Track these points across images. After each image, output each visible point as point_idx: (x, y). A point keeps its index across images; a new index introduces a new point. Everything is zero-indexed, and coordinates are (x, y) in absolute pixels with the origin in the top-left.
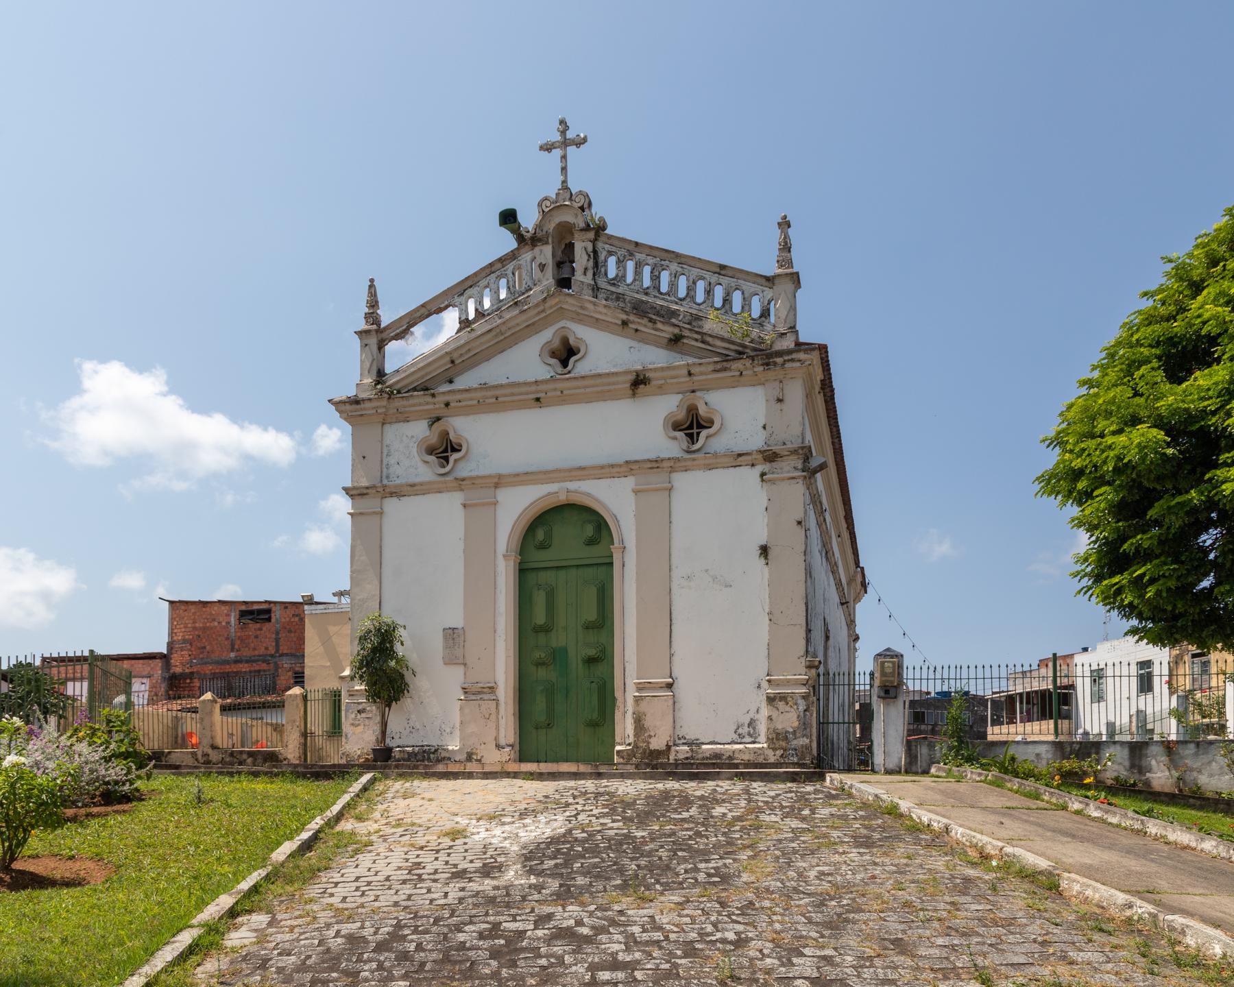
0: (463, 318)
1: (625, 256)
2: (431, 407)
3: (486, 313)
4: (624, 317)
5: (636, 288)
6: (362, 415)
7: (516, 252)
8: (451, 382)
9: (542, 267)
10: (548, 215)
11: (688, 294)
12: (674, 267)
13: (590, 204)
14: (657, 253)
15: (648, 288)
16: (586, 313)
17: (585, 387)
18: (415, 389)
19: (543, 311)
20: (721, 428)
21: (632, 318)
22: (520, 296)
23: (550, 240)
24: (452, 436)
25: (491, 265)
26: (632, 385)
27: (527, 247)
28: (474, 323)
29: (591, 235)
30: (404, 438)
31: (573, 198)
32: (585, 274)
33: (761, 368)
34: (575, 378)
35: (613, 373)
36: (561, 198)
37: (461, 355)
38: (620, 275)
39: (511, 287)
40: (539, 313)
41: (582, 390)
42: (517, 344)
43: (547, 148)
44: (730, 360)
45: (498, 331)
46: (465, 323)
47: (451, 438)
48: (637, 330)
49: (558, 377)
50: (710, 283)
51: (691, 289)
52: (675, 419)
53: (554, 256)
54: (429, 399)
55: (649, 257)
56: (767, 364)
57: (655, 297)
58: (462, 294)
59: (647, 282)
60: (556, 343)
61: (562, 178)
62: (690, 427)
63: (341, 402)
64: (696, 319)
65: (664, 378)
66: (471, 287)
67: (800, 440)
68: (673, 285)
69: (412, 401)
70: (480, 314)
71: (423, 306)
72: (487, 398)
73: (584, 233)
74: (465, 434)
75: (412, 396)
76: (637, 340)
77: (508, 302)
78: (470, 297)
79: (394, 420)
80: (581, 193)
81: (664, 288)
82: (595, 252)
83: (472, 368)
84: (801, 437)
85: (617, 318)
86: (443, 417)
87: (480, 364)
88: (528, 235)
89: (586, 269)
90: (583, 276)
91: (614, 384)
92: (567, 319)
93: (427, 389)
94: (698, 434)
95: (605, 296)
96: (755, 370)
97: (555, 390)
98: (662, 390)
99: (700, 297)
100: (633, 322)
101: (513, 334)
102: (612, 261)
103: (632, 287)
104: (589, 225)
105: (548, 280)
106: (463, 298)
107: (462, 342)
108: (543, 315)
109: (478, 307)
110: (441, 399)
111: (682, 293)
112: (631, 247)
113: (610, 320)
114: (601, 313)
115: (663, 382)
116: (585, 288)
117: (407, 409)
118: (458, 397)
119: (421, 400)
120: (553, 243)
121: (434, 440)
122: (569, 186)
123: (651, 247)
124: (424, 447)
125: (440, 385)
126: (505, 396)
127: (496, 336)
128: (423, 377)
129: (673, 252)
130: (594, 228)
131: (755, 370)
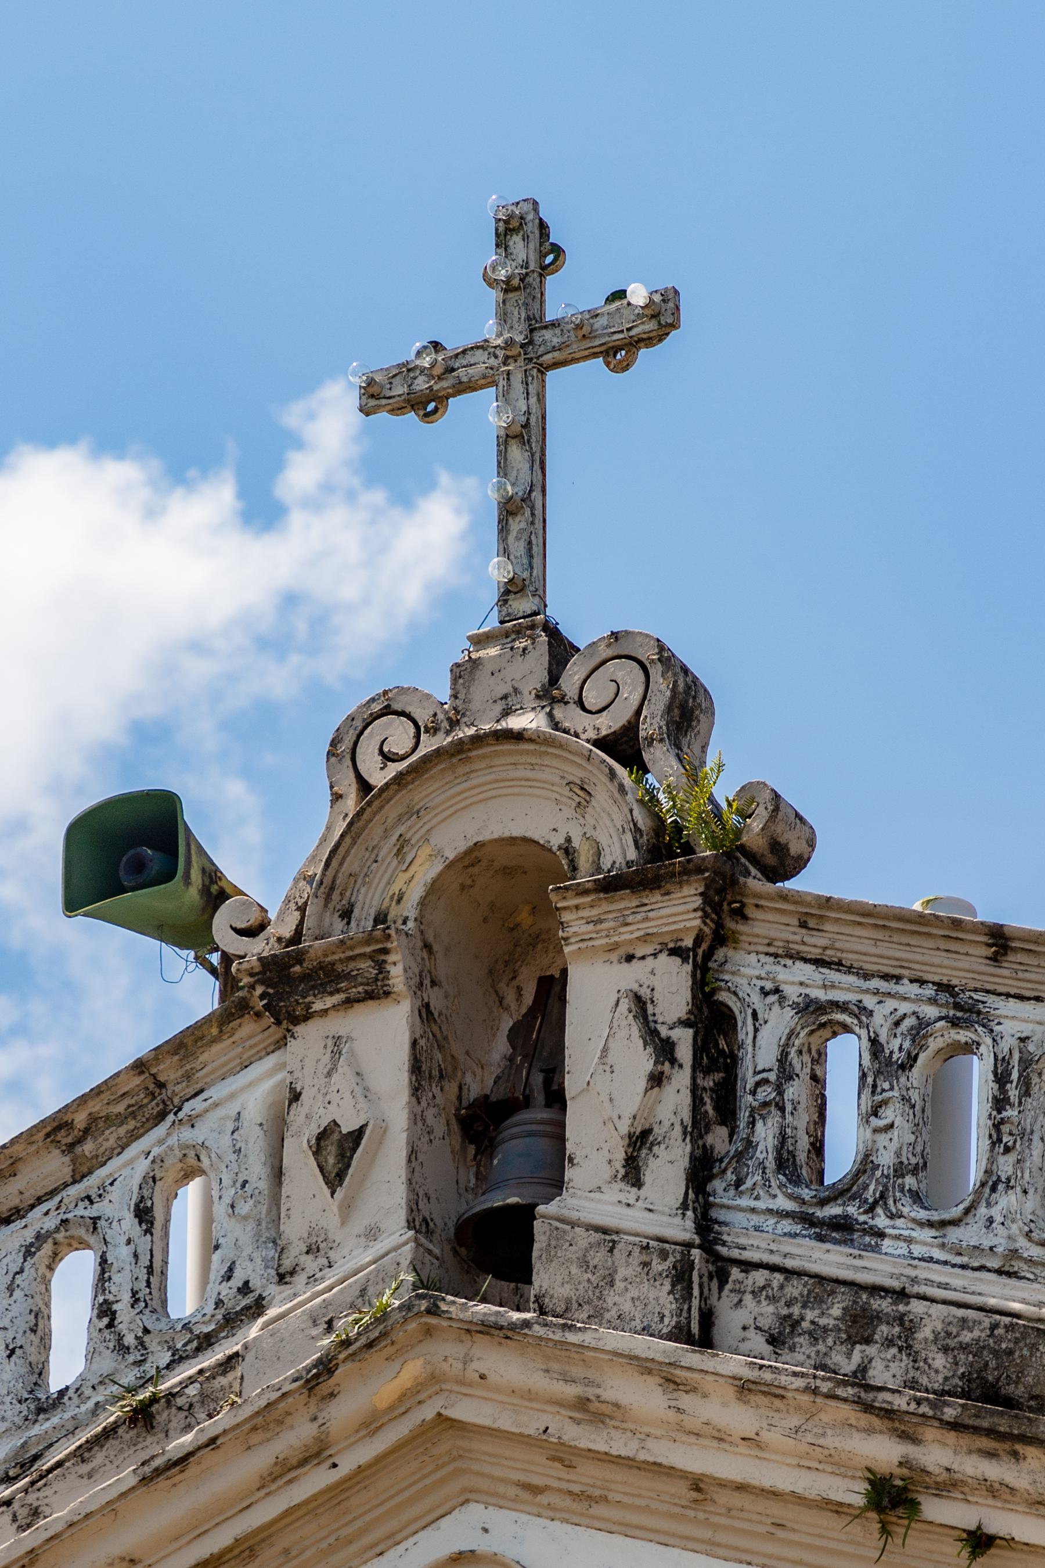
1: (920, 1031)
7: (168, 1071)
10: (392, 810)
16: (620, 1445)
22: (178, 1359)
23: (397, 974)
38: (886, 1159)
39: (123, 1308)
73: (626, 901)
92: (494, 1499)
95: (767, 1313)
105: (372, 1234)
116: (627, 1269)
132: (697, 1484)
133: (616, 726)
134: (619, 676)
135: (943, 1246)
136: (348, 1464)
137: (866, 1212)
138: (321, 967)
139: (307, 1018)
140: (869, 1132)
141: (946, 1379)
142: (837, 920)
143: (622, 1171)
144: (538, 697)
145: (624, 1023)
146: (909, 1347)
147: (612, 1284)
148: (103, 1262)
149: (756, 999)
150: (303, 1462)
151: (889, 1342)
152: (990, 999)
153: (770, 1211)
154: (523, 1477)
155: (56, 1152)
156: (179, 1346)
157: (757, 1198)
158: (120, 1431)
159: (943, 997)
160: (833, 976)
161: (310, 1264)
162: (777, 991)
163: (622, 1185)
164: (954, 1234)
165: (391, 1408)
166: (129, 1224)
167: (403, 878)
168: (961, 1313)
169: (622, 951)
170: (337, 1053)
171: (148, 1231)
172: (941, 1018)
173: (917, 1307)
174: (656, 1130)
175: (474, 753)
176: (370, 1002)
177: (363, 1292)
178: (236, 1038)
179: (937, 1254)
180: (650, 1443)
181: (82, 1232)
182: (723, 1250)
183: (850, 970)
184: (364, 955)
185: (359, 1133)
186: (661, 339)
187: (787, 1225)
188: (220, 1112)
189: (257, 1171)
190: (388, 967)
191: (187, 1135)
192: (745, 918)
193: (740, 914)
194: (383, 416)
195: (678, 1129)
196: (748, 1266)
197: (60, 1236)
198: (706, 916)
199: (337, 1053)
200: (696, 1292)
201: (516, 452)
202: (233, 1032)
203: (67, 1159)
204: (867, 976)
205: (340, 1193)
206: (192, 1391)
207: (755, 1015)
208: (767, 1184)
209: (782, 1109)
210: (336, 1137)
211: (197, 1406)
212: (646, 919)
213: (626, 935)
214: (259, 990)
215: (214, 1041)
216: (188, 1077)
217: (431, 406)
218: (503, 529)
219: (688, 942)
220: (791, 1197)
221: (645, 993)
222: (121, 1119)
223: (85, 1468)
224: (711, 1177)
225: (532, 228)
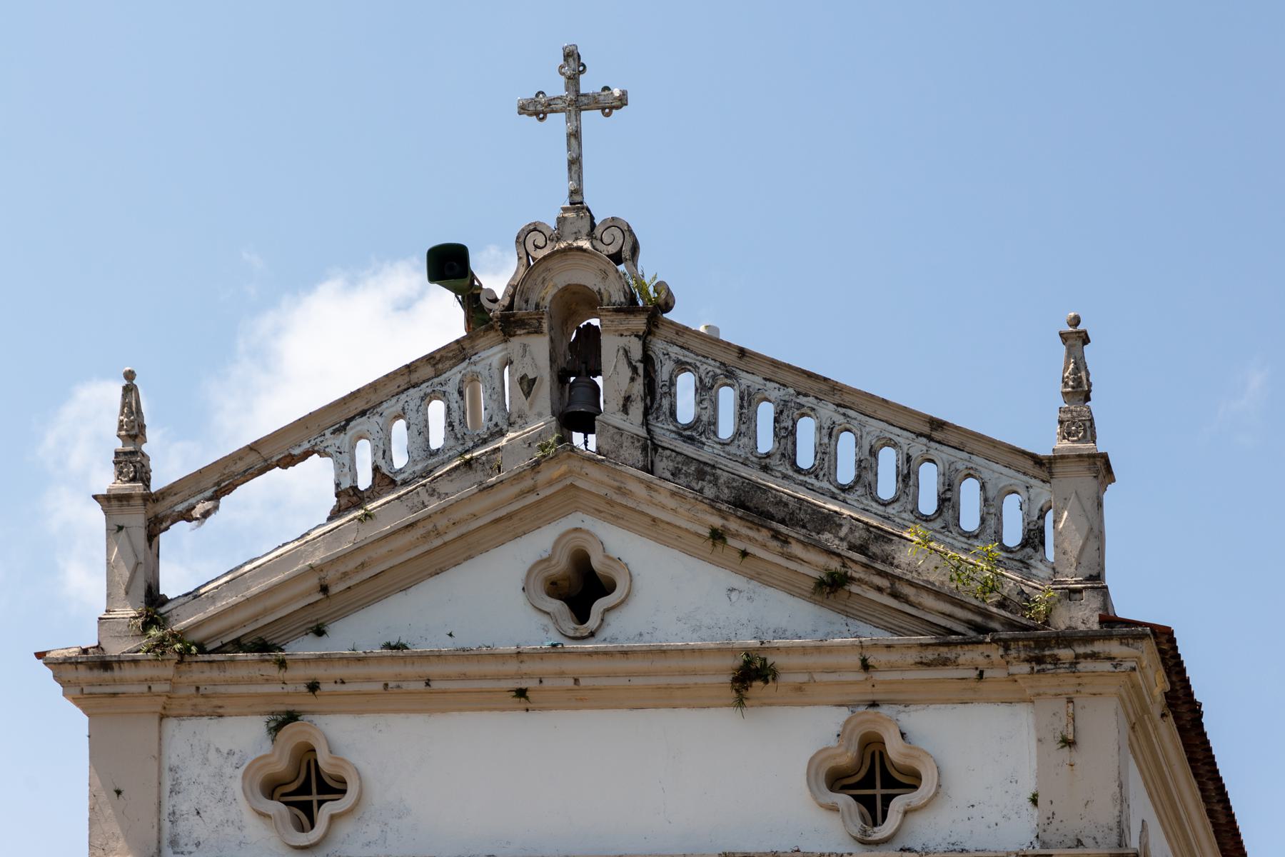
0: (346, 484)
1: (715, 377)
2: (276, 688)
3: (399, 479)
4: (717, 522)
5: (742, 452)
6: (114, 695)
7: (467, 345)
8: (320, 632)
9: (527, 385)
11: (858, 477)
12: (828, 411)
13: (635, 249)
14: (789, 378)
15: (768, 455)
16: (631, 504)
17: (630, 674)
18: (238, 645)
19: (532, 490)
20: (936, 794)
21: (733, 525)
22: (476, 446)
23: (545, 326)
24: (323, 759)
25: (410, 368)
26: (735, 680)
27: (492, 334)
28: (372, 500)
29: (639, 323)
30: (212, 755)
31: (598, 232)
32: (625, 409)
33: (1025, 668)
34: (606, 653)
35: (693, 650)
36: (568, 229)
37: (345, 574)
38: (705, 419)
39: (456, 424)
40: (523, 494)
41: (622, 682)
42: (470, 557)
43: (537, 109)
44: (956, 644)
45: (430, 527)
46: (349, 498)
47: (321, 763)
48: (744, 554)
49: (571, 645)
50: (909, 458)
51: (866, 466)
52: (832, 764)
53: (553, 360)
54: (273, 671)
55: (770, 385)
56: (1040, 660)
57: (785, 477)
58: (342, 429)
59: (766, 442)
60: (561, 565)
61: (572, 185)
62: (868, 782)
63: (67, 661)
64: (877, 538)
65: (809, 671)
66: (363, 413)
67: (1114, 838)
68: (826, 454)
69: (231, 673)
70: (384, 479)
71: (253, 448)
72: (406, 679)
73: (622, 316)
74: (353, 758)
75: (232, 661)
76: (744, 574)
77: (450, 459)
78: (361, 438)
79: (189, 712)
80: (613, 223)
81: (806, 459)
82: (647, 359)
83: (368, 604)
84: (1116, 831)
85: (701, 523)
86: (301, 713)
87: (386, 596)
88: (496, 310)
89: (627, 399)
90: (620, 415)
91: (694, 673)
93: (263, 646)
94: (887, 800)
95: (671, 465)
96: (1013, 669)
97: (561, 674)
98: (801, 695)
99: (887, 487)
100: (736, 535)
101: (461, 537)
102: (686, 385)
103: (732, 449)
104: (633, 300)
106: (343, 440)
107: (347, 546)
108: (532, 498)
109: (381, 463)
110: (301, 674)
111: (846, 473)
112: (731, 359)
113: (684, 524)
114: (664, 507)
115: (803, 678)
117: (222, 689)
118: (339, 671)
119: (255, 672)
120: (551, 329)
121: (281, 765)
122: (588, 202)
123: (775, 364)
124: (259, 779)
125: (296, 636)
126: (447, 678)
127: (425, 537)
128: (255, 618)
129: (826, 379)
130: (644, 310)
131: (1013, 669)
132: (654, 520)
133: (614, 251)
134: (615, 233)
135: (724, 451)
136: (542, 495)
137: (699, 435)
138: (520, 320)
139: (514, 336)
140: (699, 409)
141: (728, 497)
142: (688, 335)
143: (622, 409)
144: (587, 235)
145: (621, 358)
146: (716, 485)
147: (622, 447)
148: (449, 411)
149: (661, 355)
150: (528, 492)
151: (710, 482)
152: (738, 371)
153: (668, 429)
154: (597, 507)
155: (430, 366)
156: (476, 440)
157: (663, 424)
158: (461, 467)
159: (722, 367)
160: (687, 353)
161: (520, 422)
162: (668, 354)
163: (621, 413)
164: (727, 448)
165: (557, 479)
166: (456, 395)
167: (544, 292)
168: (733, 476)
169: (619, 332)
170: (525, 351)
171: (462, 399)
172: (722, 374)
173: (719, 472)
174: (632, 396)
175: (569, 253)
176: (536, 334)
177: (540, 435)
178: (489, 337)
179: (722, 454)
180: (640, 505)
181: (440, 395)
182: (656, 442)
183: (692, 352)
184: (534, 318)
185: (534, 380)
186: (621, 108)
187: (673, 435)
188: (484, 362)
189: (497, 384)
190: (542, 324)
191: (474, 368)
192: (658, 328)
193: (657, 326)
194: (525, 116)
195: (639, 398)
196: (664, 448)
197: (432, 395)
198: (647, 326)
199: (525, 351)
200: (649, 455)
201: (573, 140)
202: (487, 335)
203: (433, 369)
204: (697, 355)
205: (529, 399)
206: (484, 458)
207: (661, 361)
208: (666, 420)
209: (671, 395)
210: (526, 379)
211: (486, 464)
212: (628, 324)
213: (621, 327)
214: (499, 324)
215: (482, 337)
216: (473, 347)
217: (541, 116)
218: (570, 169)
219: (641, 333)
220: (674, 426)
221: (627, 348)
222: (451, 358)
223: (450, 478)
224: (649, 415)
225: (576, 56)
